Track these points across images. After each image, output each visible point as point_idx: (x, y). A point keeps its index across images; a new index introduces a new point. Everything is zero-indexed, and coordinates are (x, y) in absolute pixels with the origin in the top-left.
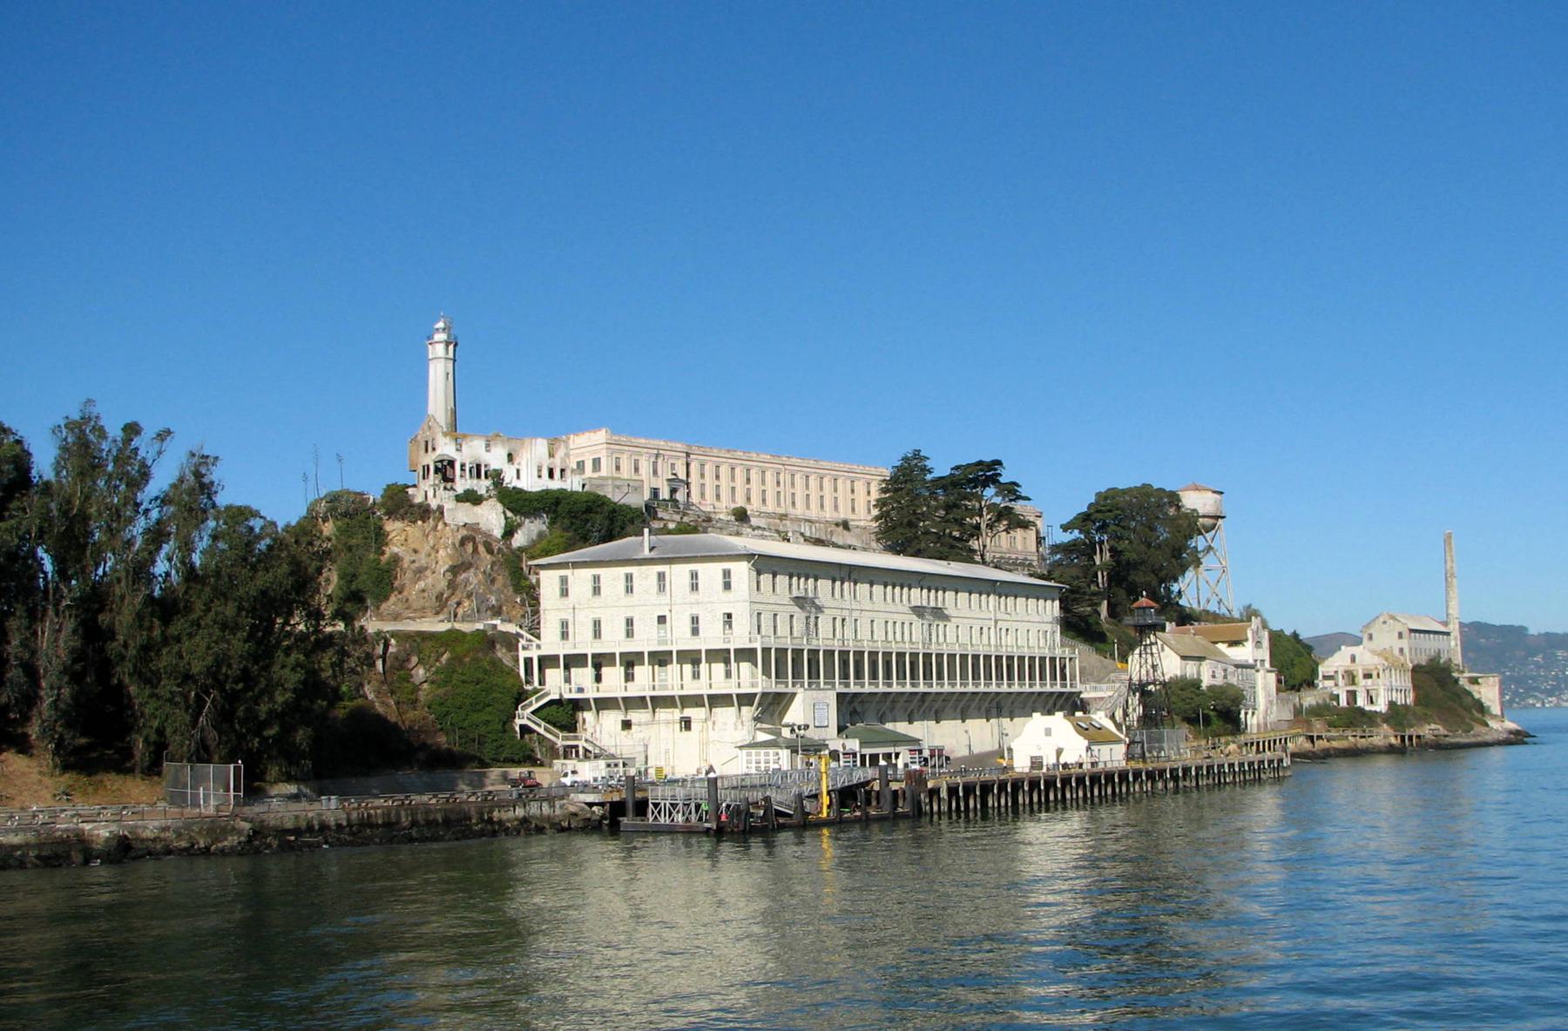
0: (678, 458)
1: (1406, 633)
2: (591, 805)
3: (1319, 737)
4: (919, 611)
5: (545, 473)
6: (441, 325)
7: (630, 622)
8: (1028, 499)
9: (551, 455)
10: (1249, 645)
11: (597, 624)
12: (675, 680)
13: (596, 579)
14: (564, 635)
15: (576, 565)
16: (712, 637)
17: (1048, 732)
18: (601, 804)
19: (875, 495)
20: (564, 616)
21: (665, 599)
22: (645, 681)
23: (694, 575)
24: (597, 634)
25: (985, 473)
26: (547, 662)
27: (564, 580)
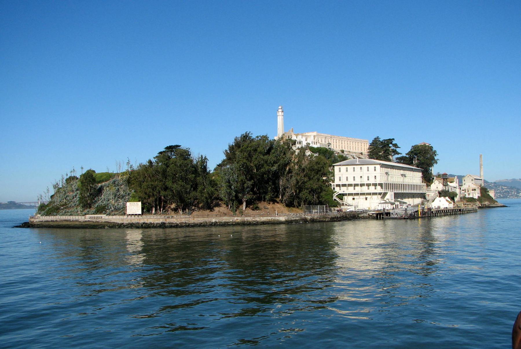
0: (329, 138)
1: (473, 180)
2: (373, 214)
3: (465, 204)
4: (402, 175)
5: (313, 143)
6: (280, 107)
7: (354, 177)
8: (400, 148)
9: (314, 139)
10: (455, 183)
11: (347, 178)
12: (365, 189)
13: (347, 168)
14: (340, 180)
15: (343, 165)
16: (372, 181)
17: (440, 201)
18: (375, 214)
19: (368, 147)
20: (340, 176)
21: (362, 173)
22: (358, 190)
23: (368, 168)
24: (347, 180)
25: (390, 141)
26: (338, 185)
27: (340, 168)
